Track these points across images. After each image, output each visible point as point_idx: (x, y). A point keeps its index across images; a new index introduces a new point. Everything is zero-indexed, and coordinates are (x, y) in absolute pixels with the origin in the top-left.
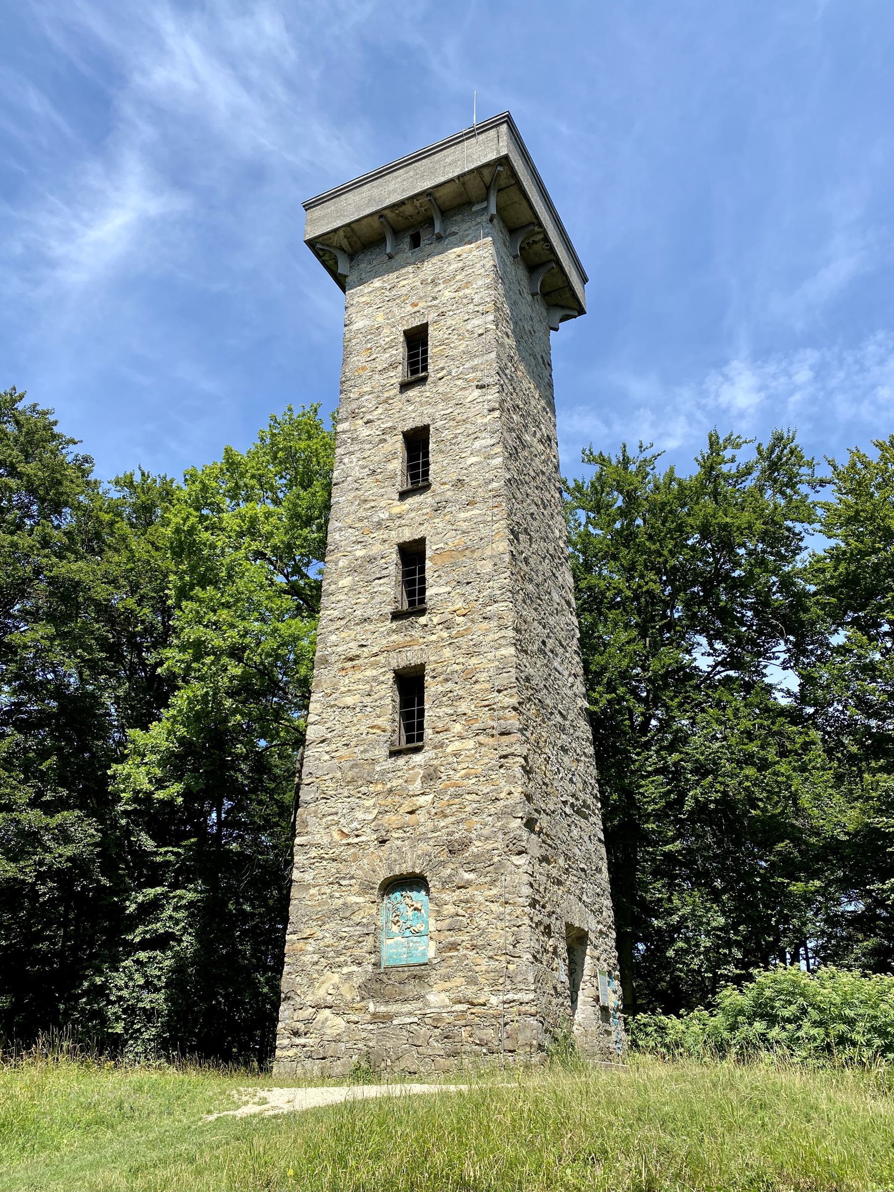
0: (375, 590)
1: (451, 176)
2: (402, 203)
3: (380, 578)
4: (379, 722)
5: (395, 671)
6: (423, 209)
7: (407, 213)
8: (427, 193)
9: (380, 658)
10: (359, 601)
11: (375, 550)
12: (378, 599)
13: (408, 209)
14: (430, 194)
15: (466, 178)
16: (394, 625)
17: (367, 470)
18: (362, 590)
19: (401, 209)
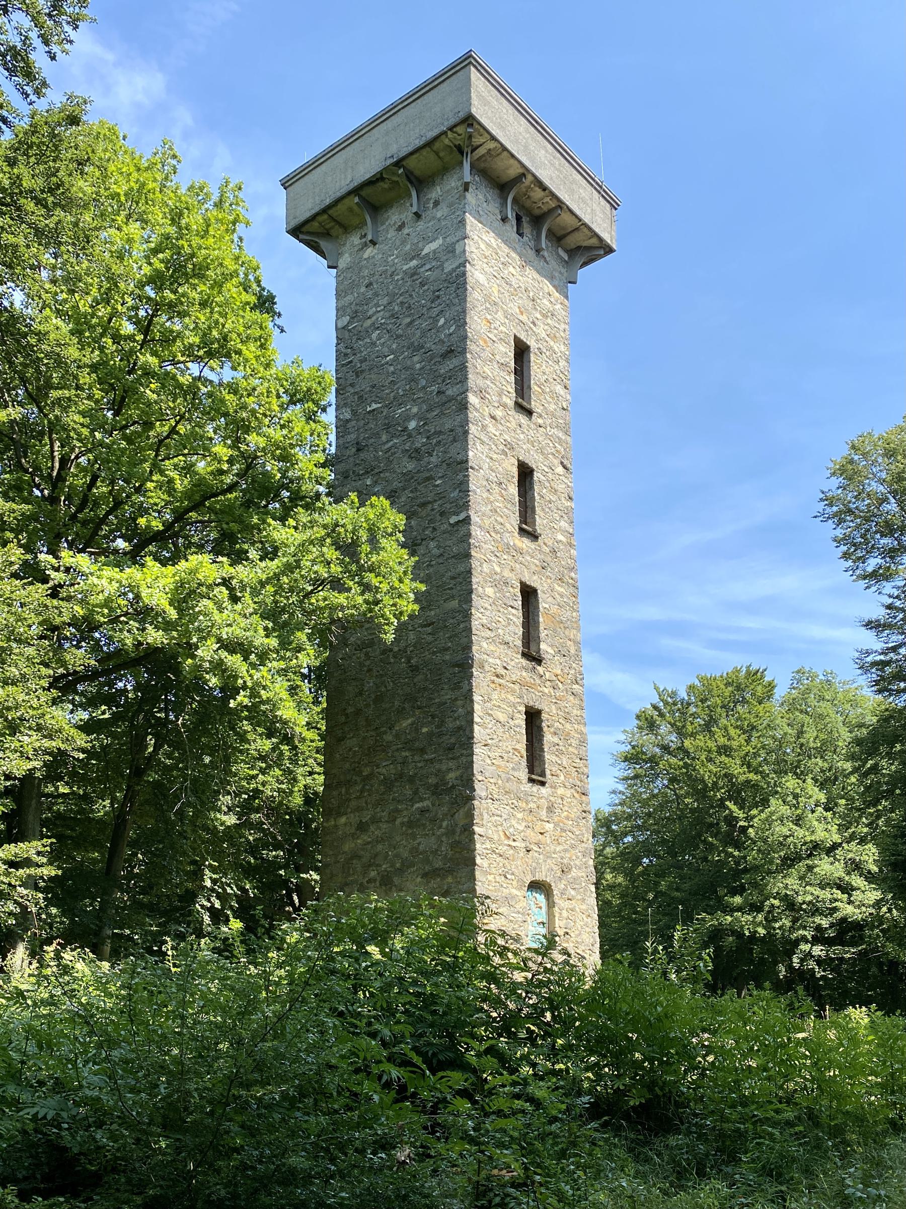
0: (511, 617)
1: (582, 216)
2: (544, 188)
3: (512, 607)
4: (517, 747)
5: (526, 707)
6: (540, 205)
7: (532, 194)
8: (561, 205)
9: (517, 687)
10: (500, 619)
11: (507, 573)
12: (512, 628)
13: (538, 194)
14: (561, 208)
15: (585, 230)
16: (524, 662)
17: (494, 474)
18: (502, 610)
19: (537, 189)
